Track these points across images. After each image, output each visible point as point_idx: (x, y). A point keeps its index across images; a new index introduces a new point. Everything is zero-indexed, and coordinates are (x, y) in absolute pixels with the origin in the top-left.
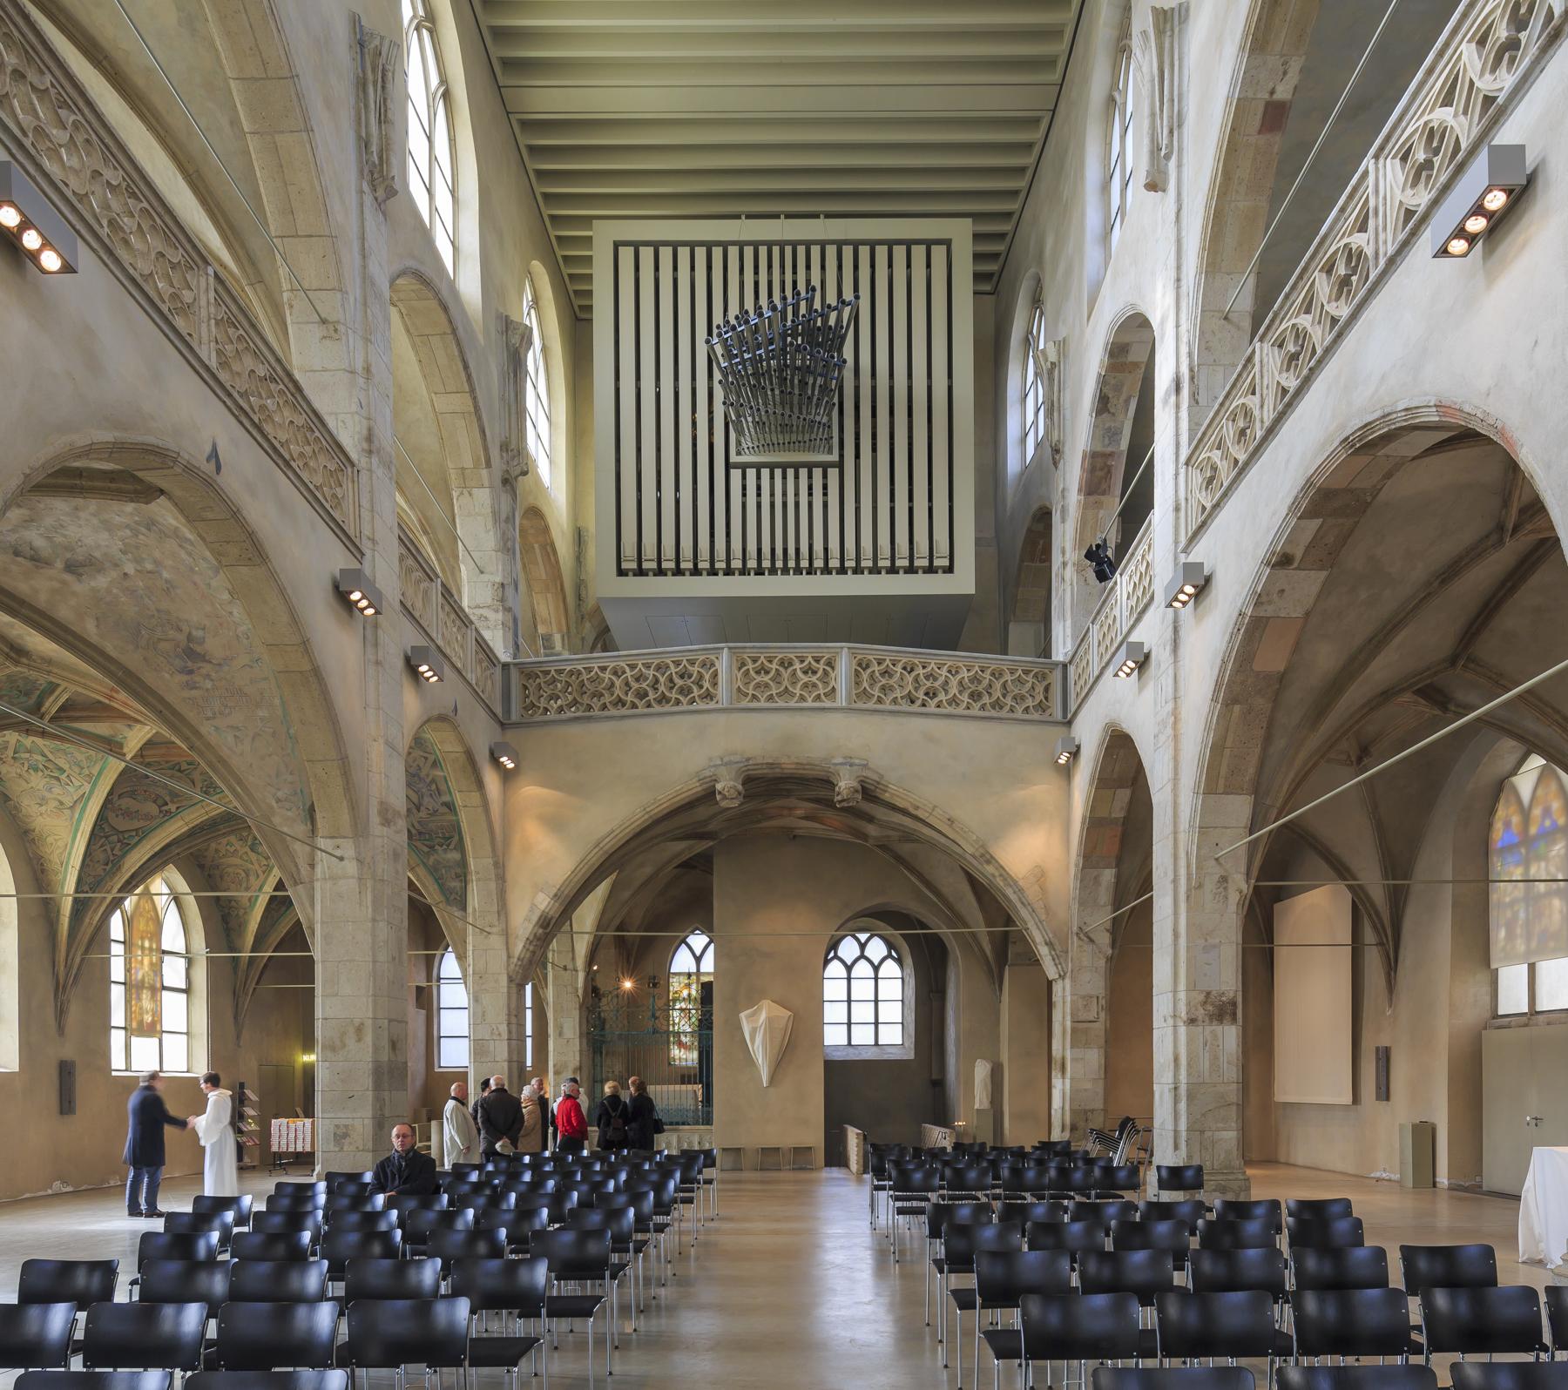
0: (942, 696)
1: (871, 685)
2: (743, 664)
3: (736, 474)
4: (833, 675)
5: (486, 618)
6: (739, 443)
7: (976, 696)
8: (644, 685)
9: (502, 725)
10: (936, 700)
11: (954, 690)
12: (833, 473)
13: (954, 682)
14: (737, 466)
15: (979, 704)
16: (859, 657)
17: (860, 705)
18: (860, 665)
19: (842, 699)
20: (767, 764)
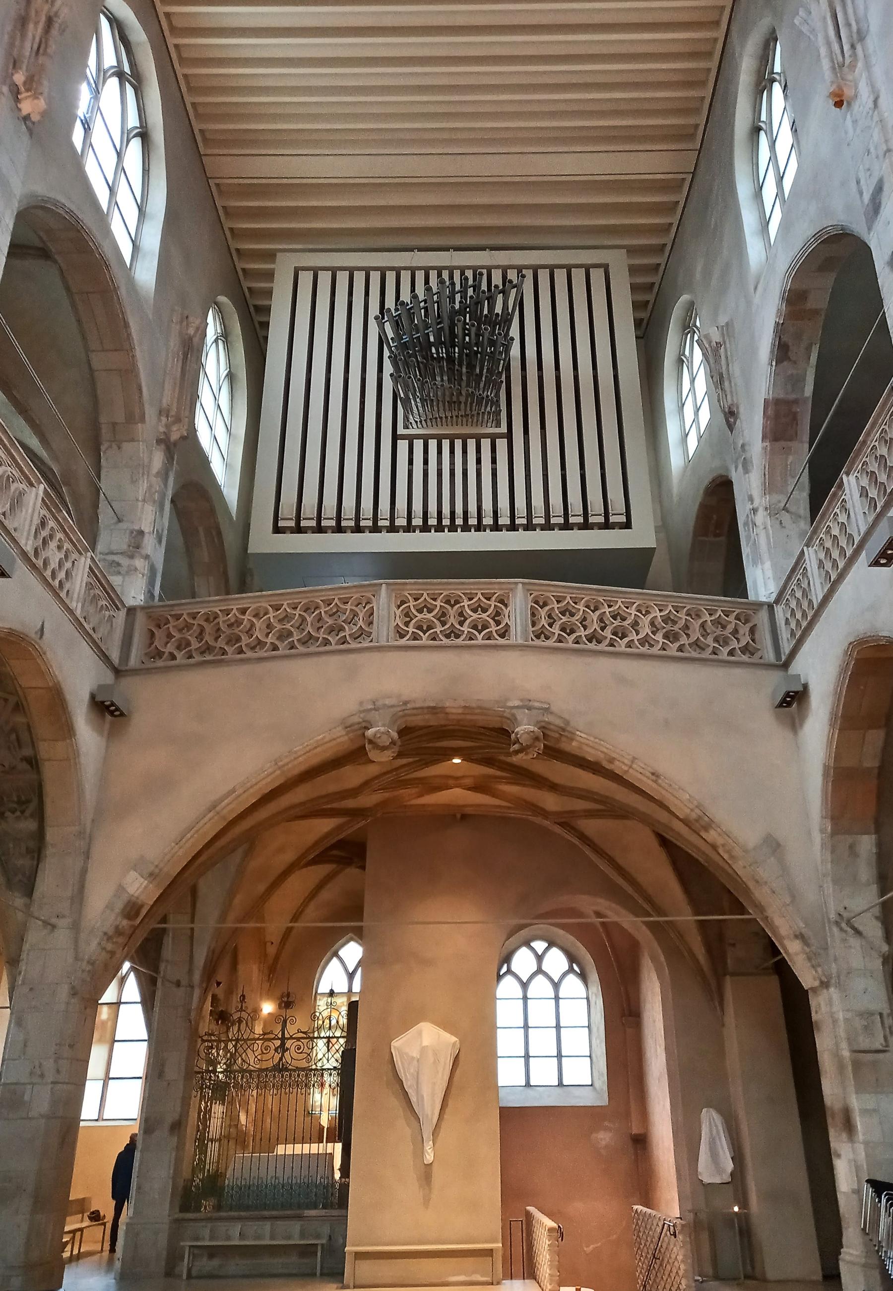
0: (633, 636)
1: (551, 625)
2: (403, 602)
3: (403, 445)
4: (506, 612)
5: (119, 564)
6: (406, 418)
7: (671, 636)
8: (288, 626)
9: (118, 672)
10: (626, 640)
11: (646, 630)
12: (502, 444)
13: (645, 621)
14: (404, 437)
15: (677, 645)
16: (535, 594)
17: (537, 642)
18: (536, 602)
19: (516, 636)
20: (428, 708)
